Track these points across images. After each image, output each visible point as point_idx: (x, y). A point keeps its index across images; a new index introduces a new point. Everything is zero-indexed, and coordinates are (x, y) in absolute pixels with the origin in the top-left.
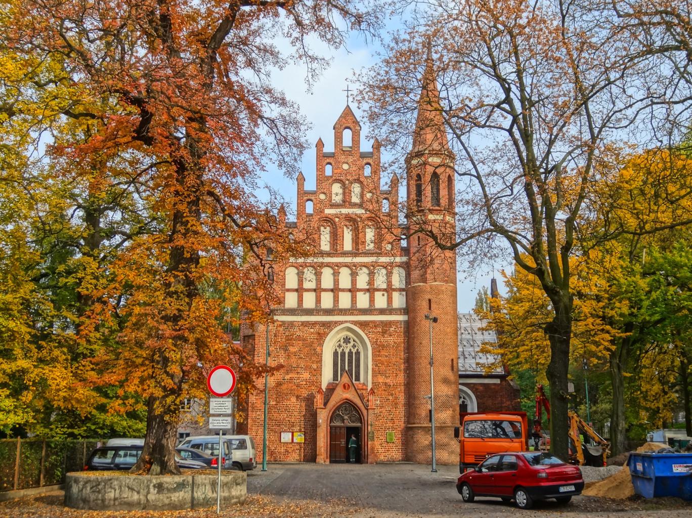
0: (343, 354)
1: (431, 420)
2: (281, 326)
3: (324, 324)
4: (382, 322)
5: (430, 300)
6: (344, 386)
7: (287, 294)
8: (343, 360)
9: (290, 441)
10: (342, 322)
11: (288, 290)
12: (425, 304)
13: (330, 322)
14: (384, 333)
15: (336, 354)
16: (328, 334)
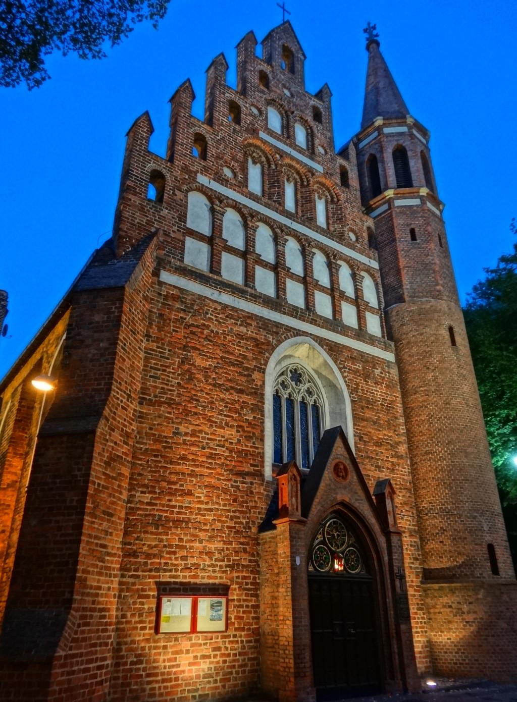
0: (290, 401)
1: (495, 570)
2: (175, 298)
3: (265, 324)
4: (362, 354)
5: (451, 329)
6: (336, 468)
7: (189, 242)
8: (291, 418)
9: (187, 627)
10: (298, 333)
11: (192, 233)
12: (445, 334)
13: (277, 325)
14: (367, 376)
15: (277, 398)
16: (273, 349)
